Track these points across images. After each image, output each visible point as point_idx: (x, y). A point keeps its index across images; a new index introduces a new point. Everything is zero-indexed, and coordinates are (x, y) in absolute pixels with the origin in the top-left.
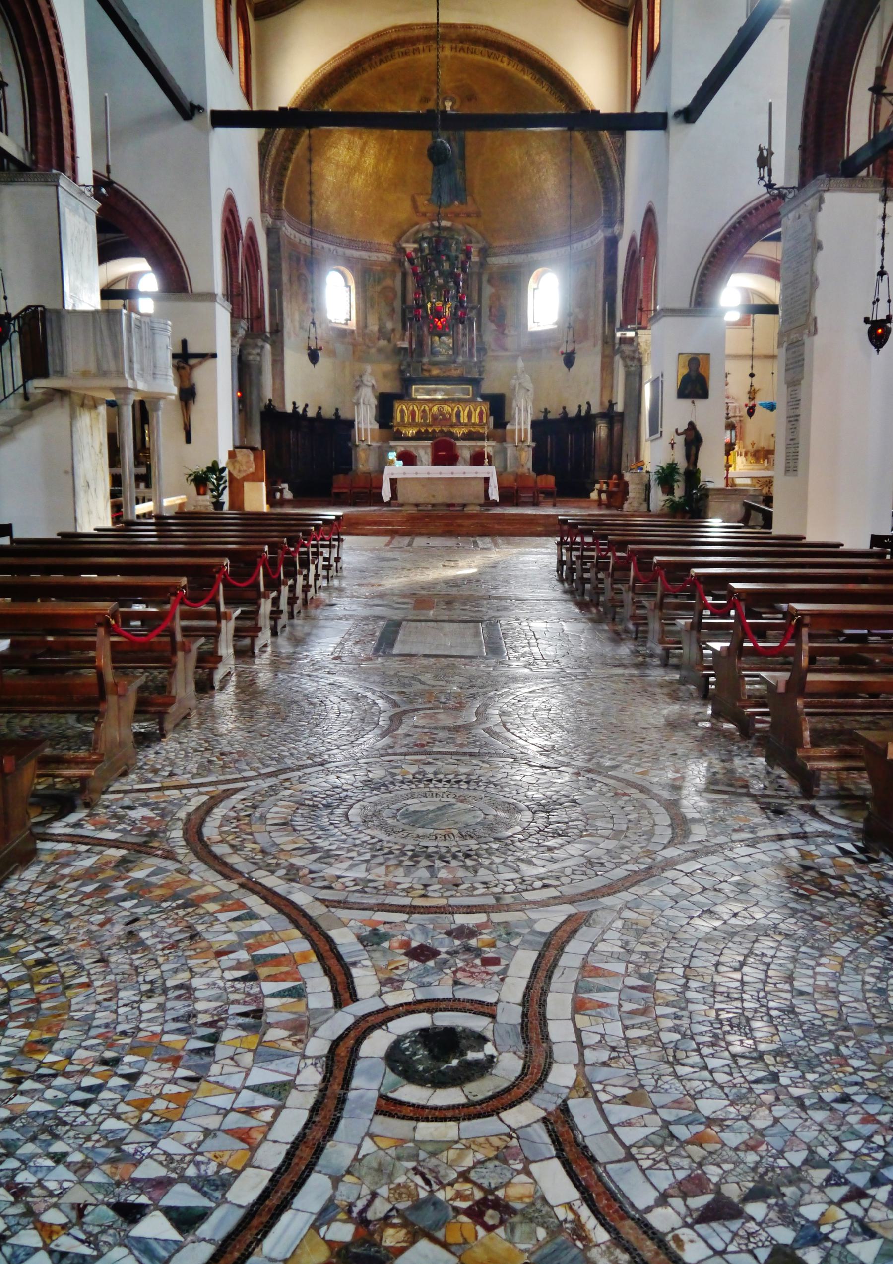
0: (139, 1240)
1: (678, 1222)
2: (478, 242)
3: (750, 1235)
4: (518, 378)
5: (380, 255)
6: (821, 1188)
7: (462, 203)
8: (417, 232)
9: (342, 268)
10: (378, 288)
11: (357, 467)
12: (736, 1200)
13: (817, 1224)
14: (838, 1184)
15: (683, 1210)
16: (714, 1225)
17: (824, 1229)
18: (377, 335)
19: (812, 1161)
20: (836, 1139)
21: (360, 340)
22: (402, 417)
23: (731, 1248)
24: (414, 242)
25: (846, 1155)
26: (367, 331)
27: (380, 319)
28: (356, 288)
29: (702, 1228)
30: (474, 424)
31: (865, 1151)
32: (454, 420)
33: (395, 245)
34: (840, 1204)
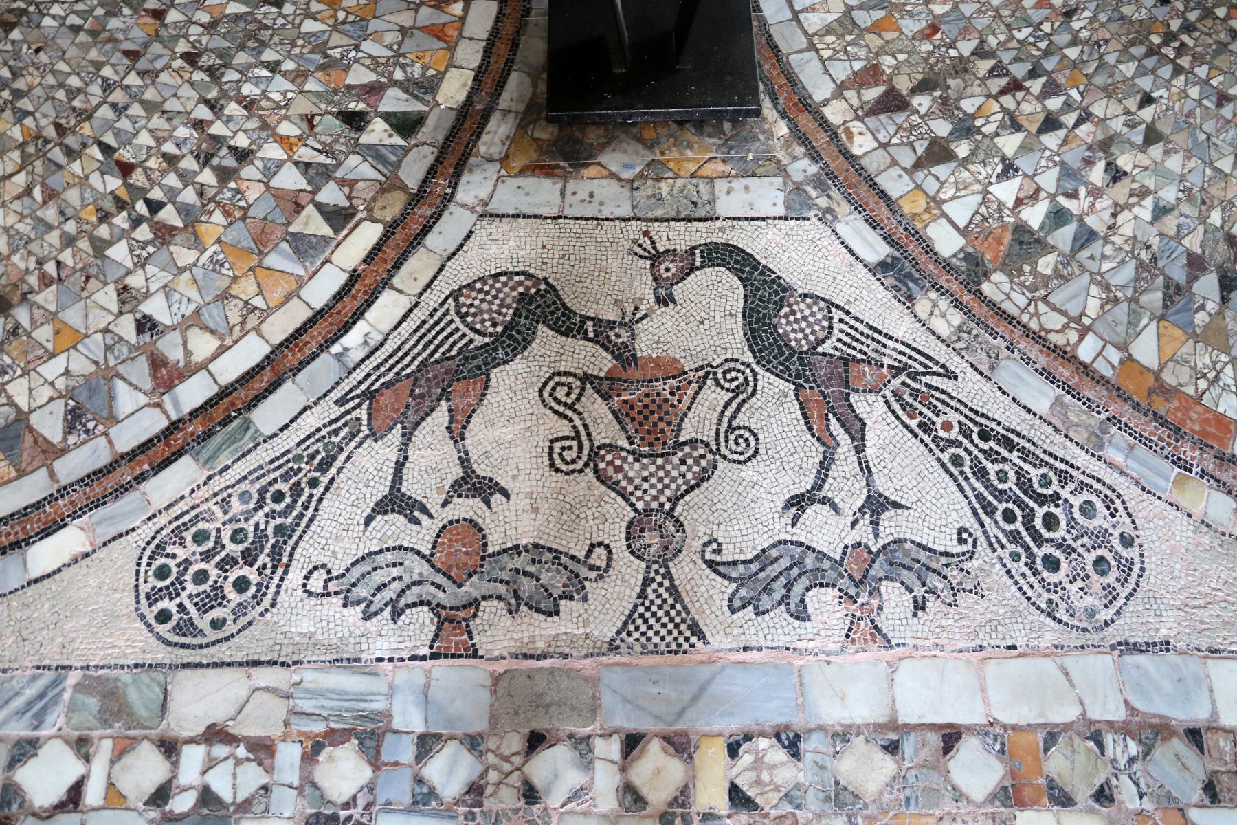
0: (369, 147)
1: (850, 116)
3: (913, 127)
6: (983, 80)
12: (905, 93)
13: (973, 117)
14: (999, 76)
15: (855, 103)
16: (882, 117)
17: (978, 123)
19: (981, 52)
20: (1008, 26)
23: (895, 141)
25: (1014, 44)
29: (872, 121)
31: (1031, 40)
34: (996, 97)
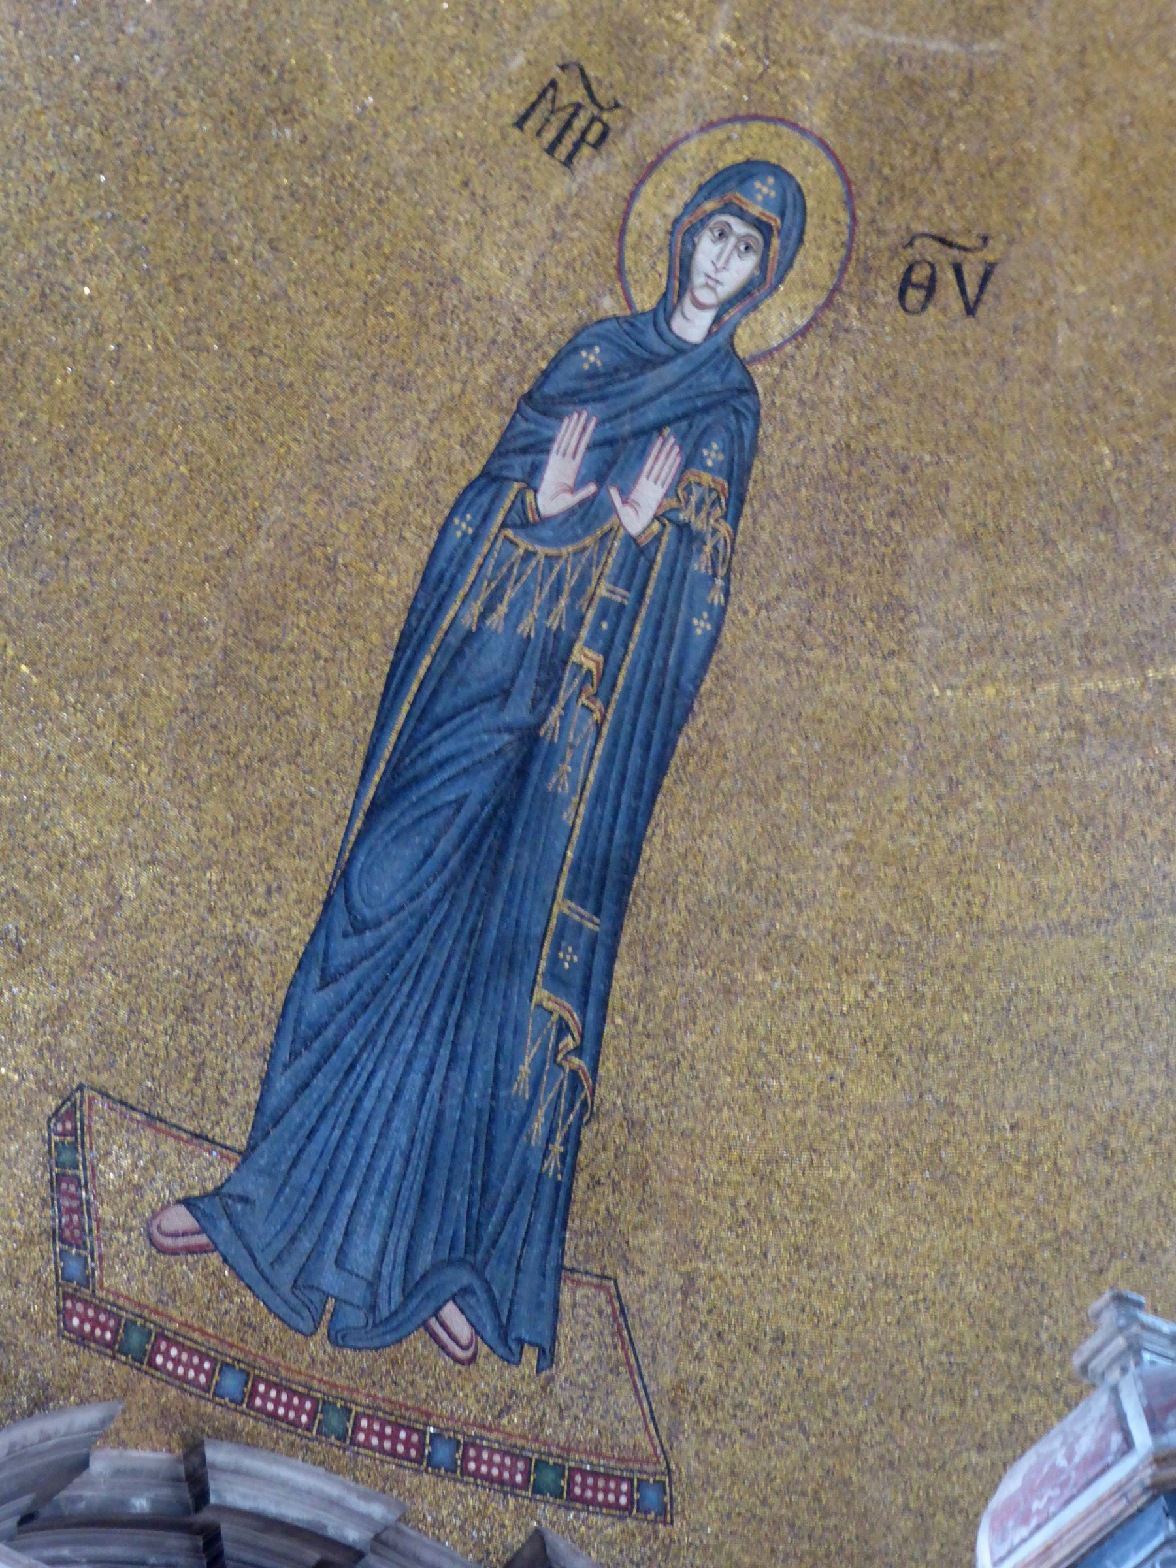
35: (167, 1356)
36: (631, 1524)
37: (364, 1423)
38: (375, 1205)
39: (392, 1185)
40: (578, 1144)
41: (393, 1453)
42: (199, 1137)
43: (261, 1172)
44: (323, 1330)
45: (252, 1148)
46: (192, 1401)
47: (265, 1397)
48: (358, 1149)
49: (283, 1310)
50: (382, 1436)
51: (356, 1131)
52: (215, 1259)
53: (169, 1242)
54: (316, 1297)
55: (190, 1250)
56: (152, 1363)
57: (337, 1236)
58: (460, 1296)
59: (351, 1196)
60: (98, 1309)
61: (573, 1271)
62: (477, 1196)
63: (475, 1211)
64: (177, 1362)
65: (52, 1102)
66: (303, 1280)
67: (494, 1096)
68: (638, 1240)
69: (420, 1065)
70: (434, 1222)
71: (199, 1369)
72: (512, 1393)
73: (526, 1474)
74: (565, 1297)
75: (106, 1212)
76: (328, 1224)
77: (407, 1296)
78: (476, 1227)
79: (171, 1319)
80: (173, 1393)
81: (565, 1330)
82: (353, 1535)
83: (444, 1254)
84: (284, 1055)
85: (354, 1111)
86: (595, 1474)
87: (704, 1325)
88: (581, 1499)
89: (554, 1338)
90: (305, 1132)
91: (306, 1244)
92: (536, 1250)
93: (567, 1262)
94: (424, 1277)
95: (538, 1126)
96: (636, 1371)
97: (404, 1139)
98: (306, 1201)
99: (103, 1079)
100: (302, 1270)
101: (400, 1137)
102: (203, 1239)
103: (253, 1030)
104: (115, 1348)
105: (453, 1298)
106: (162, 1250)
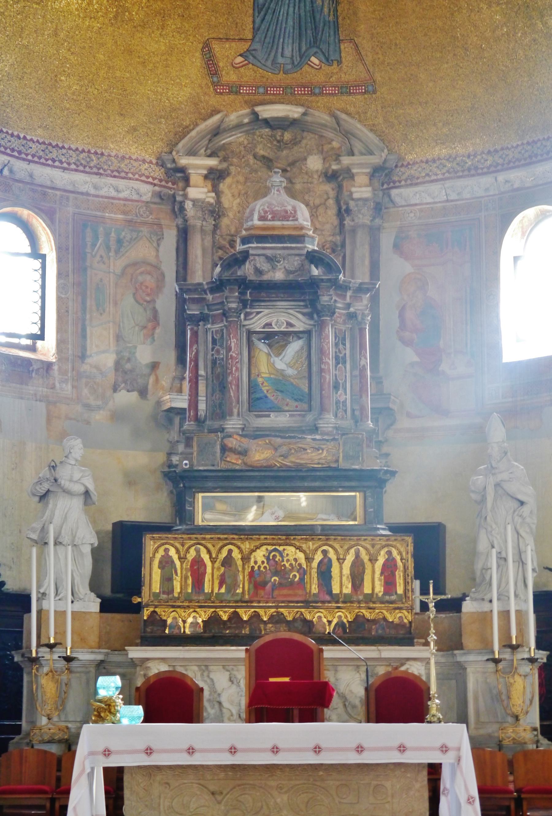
2: (371, 153)
4: (492, 470)
5: (121, 184)
7: (328, 60)
8: (216, 132)
9: (25, 213)
10: (117, 265)
11: (33, 723)
18: (111, 377)
21: (68, 389)
22: (167, 580)
24: (210, 156)
26: (85, 367)
27: (119, 338)
28: (59, 260)
30: (370, 598)
32: (315, 589)
33: (161, 163)
35: (243, 90)
36: (366, 96)
37: (296, 89)
38: (288, 41)
39: (291, 35)
40: (337, 11)
41: (305, 94)
42: (241, 39)
43: (258, 42)
44: (282, 72)
45: (254, 37)
46: (252, 97)
47: (271, 90)
48: (281, 30)
49: (270, 71)
50: (301, 91)
51: (279, 25)
52: (250, 66)
53: (238, 66)
54: (278, 65)
55: (242, 66)
56: (240, 93)
57: (280, 50)
58: (315, 55)
59: (281, 40)
60: (223, 86)
61: (342, 40)
62: (314, 30)
63: (314, 34)
64: (246, 90)
65: (201, 46)
66: (274, 62)
67: (312, 7)
68: (358, 29)
69: (292, 5)
70: (304, 40)
71: (252, 90)
72: (332, 73)
73: (338, 90)
74: (342, 47)
75: (221, 64)
76: (277, 48)
77: (301, 58)
78: (315, 38)
79: (242, 82)
80: (247, 97)
81: (343, 55)
82: (296, 116)
83: (308, 46)
84: (257, 14)
85: (277, 21)
86: (356, 86)
87: (377, 46)
88: (353, 93)
89: (341, 57)
90: (266, 30)
91: (273, 54)
92: (332, 38)
93: (341, 38)
94: (305, 52)
95: (326, 10)
96: (362, 60)
97: (292, 23)
98: (270, 46)
99: (211, 36)
100: (273, 60)
101: (290, 22)
102: (246, 62)
103: (247, 11)
104: (230, 92)
105: (313, 55)
106: (236, 68)
